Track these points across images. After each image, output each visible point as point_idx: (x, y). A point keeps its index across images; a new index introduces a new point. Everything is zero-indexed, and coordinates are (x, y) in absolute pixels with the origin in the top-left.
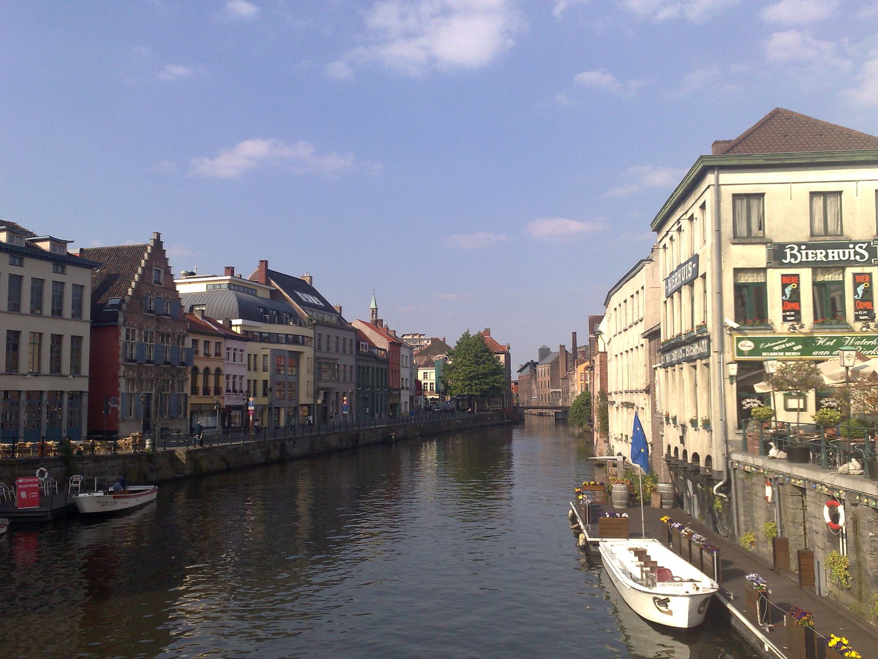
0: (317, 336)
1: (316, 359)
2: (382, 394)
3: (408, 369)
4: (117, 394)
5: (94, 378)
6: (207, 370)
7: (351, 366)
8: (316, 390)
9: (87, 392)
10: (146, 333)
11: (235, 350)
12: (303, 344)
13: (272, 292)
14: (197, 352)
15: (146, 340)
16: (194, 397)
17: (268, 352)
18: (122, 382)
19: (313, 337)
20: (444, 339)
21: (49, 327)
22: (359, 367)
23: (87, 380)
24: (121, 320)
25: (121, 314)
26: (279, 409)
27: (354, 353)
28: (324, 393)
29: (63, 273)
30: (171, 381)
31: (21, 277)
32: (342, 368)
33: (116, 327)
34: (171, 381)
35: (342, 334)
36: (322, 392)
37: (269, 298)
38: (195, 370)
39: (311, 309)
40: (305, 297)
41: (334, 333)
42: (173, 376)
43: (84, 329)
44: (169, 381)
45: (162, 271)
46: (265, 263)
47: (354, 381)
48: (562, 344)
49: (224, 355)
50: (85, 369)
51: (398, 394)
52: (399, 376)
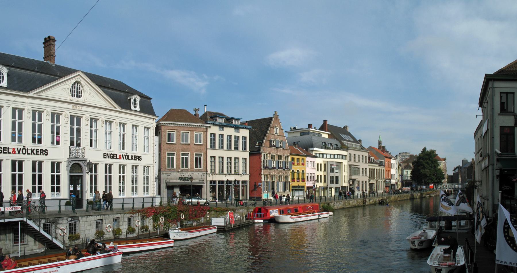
0: (349, 154)
1: (350, 166)
2: (381, 182)
3: (395, 170)
4: (261, 181)
5: (250, 176)
6: (298, 171)
7: (366, 169)
8: (349, 180)
9: (248, 181)
10: (272, 155)
11: (310, 162)
12: (342, 158)
13: (329, 134)
14: (293, 164)
15: (272, 159)
16: (293, 182)
17: (326, 163)
18: (263, 176)
19: (347, 155)
21: (233, 154)
22: (370, 169)
23: (249, 176)
24: (262, 150)
25: (262, 148)
26: (331, 188)
28: (352, 181)
29: (238, 132)
30: (283, 176)
31: (223, 135)
32: (361, 169)
33: (260, 154)
34: (283, 176)
35: (361, 153)
36: (351, 181)
37: (328, 137)
38: (293, 171)
39: (347, 142)
40: (344, 136)
41: (357, 153)
42: (284, 174)
43: (247, 155)
44: (282, 176)
45: (278, 128)
46: (325, 122)
49: (306, 164)
50: (248, 172)
51: (389, 182)
52: (390, 173)
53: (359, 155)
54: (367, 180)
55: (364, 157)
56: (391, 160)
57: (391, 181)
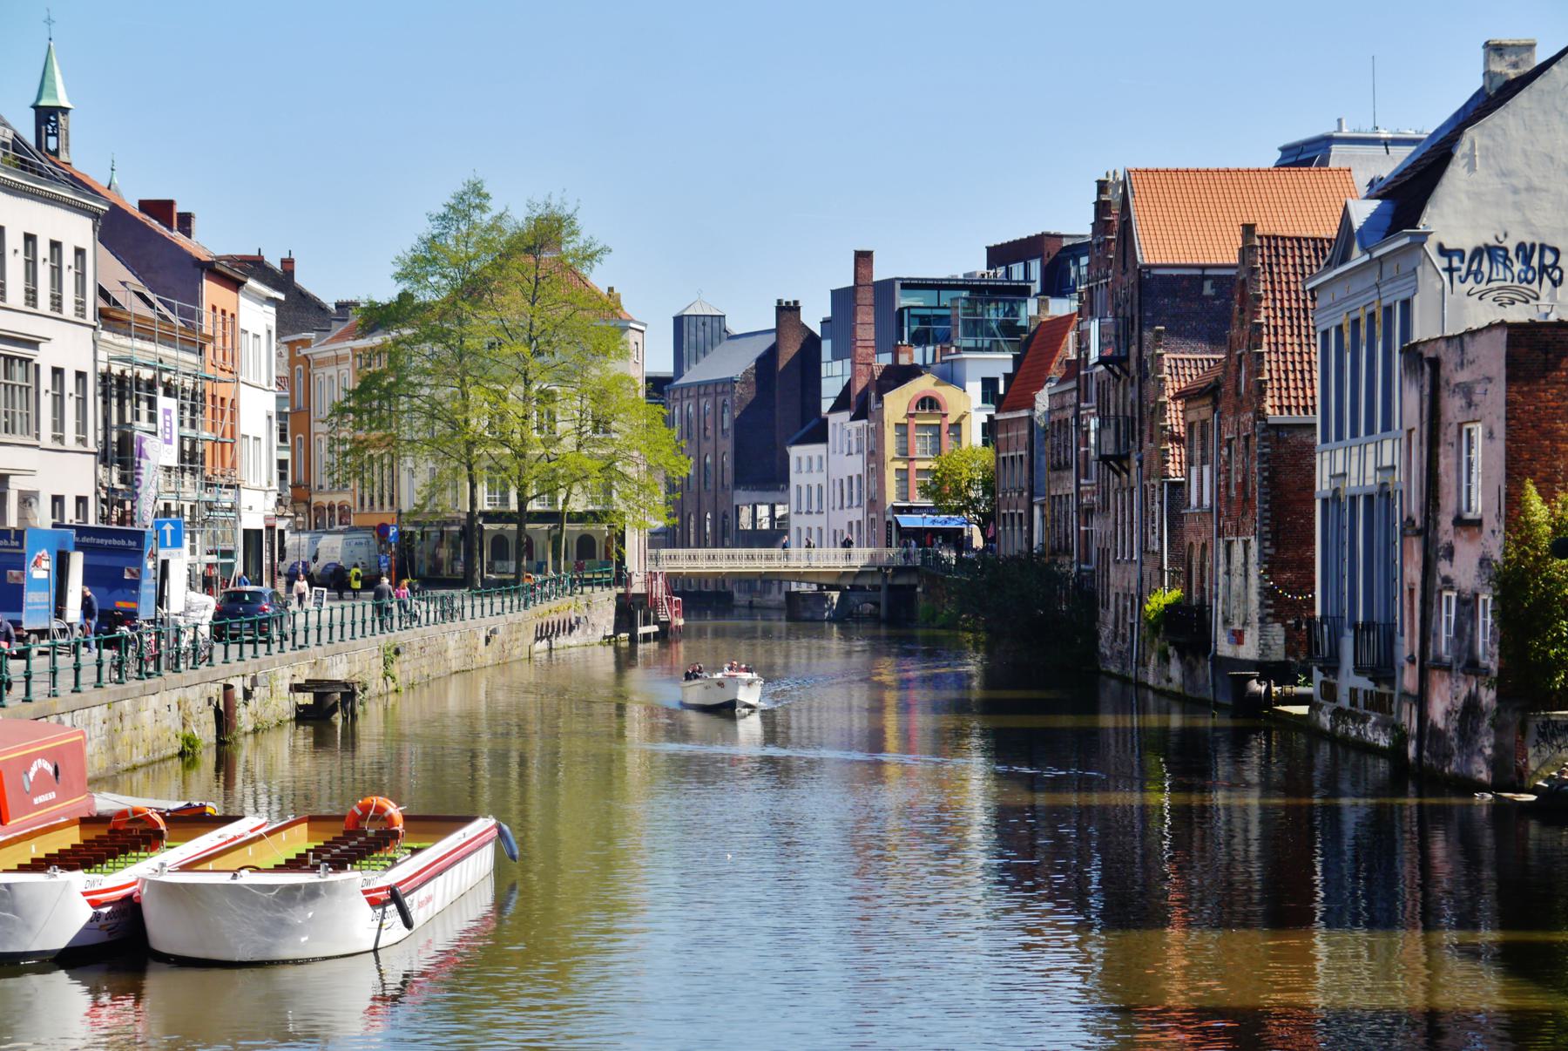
7: (80, 375)
20: (288, 263)
27: (90, 317)
47: (91, 447)
48: (786, 299)
53: (30, 239)
54: (89, 492)
55: (68, 257)
56: (243, 301)
57: (245, 503)
